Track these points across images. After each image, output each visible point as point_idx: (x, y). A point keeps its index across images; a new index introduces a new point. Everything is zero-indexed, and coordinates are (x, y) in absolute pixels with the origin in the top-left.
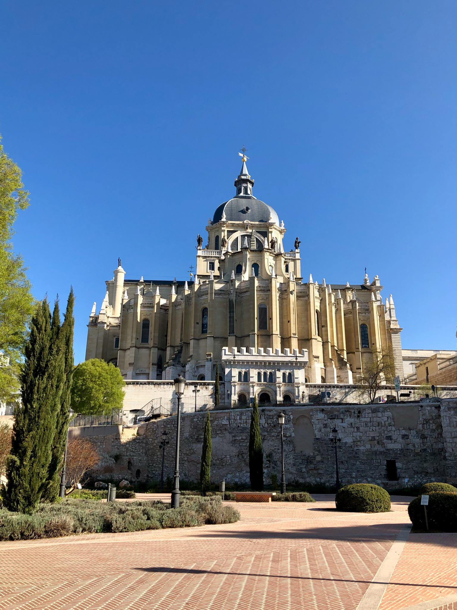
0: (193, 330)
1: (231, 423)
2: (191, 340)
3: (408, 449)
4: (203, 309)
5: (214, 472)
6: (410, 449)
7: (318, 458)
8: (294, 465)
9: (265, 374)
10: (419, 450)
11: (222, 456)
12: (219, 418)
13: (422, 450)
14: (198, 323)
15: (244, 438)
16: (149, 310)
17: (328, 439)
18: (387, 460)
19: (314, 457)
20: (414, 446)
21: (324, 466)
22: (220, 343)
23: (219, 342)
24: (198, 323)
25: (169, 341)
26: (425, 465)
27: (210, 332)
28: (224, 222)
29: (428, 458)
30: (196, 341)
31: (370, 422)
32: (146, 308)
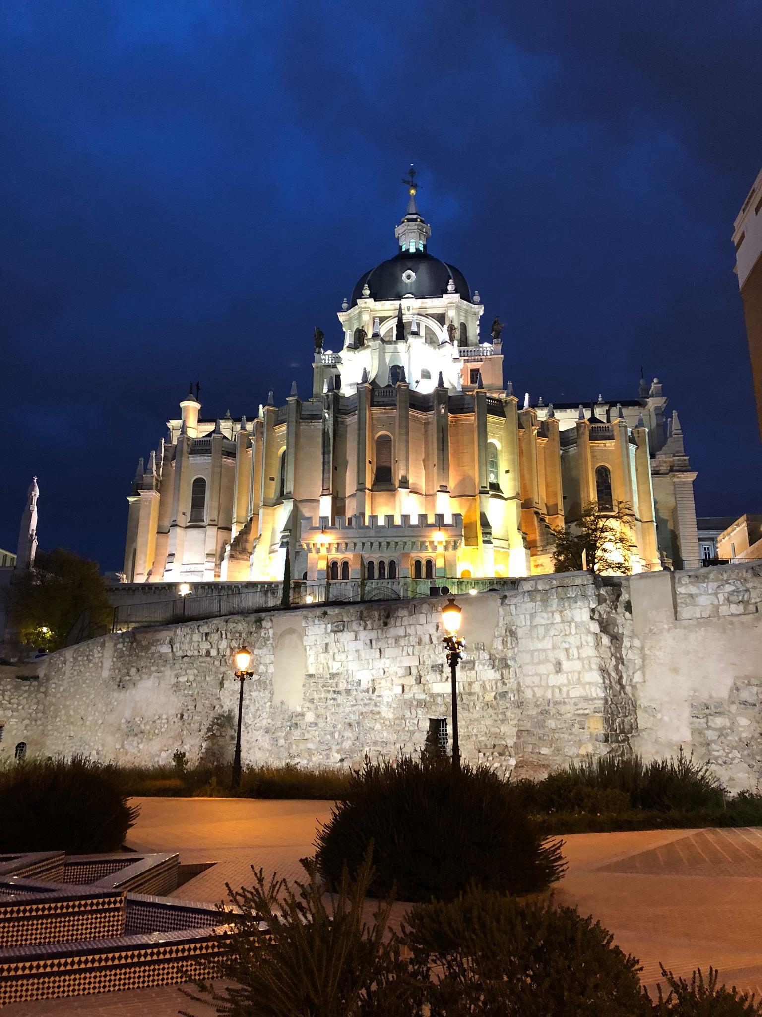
1: (174, 650)
3: (470, 694)
5: (141, 746)
6: (475, 693)
7: (310, 717)
8: (267, 732)
9: (382, 564)
10: (493, 694)
11: (155, 715)
12: (158, 640)
13: (500, 694)
14: (272, 479)
15: (192, 678)
17: (328, 676)
18: (431, 719)
19: (302, 715)
20: (484, 687)
21: (317, 733)
24: (272, 479)
25: (235, 516)
26: (503, 729)
29: (508, 714)
31: (405, 636)
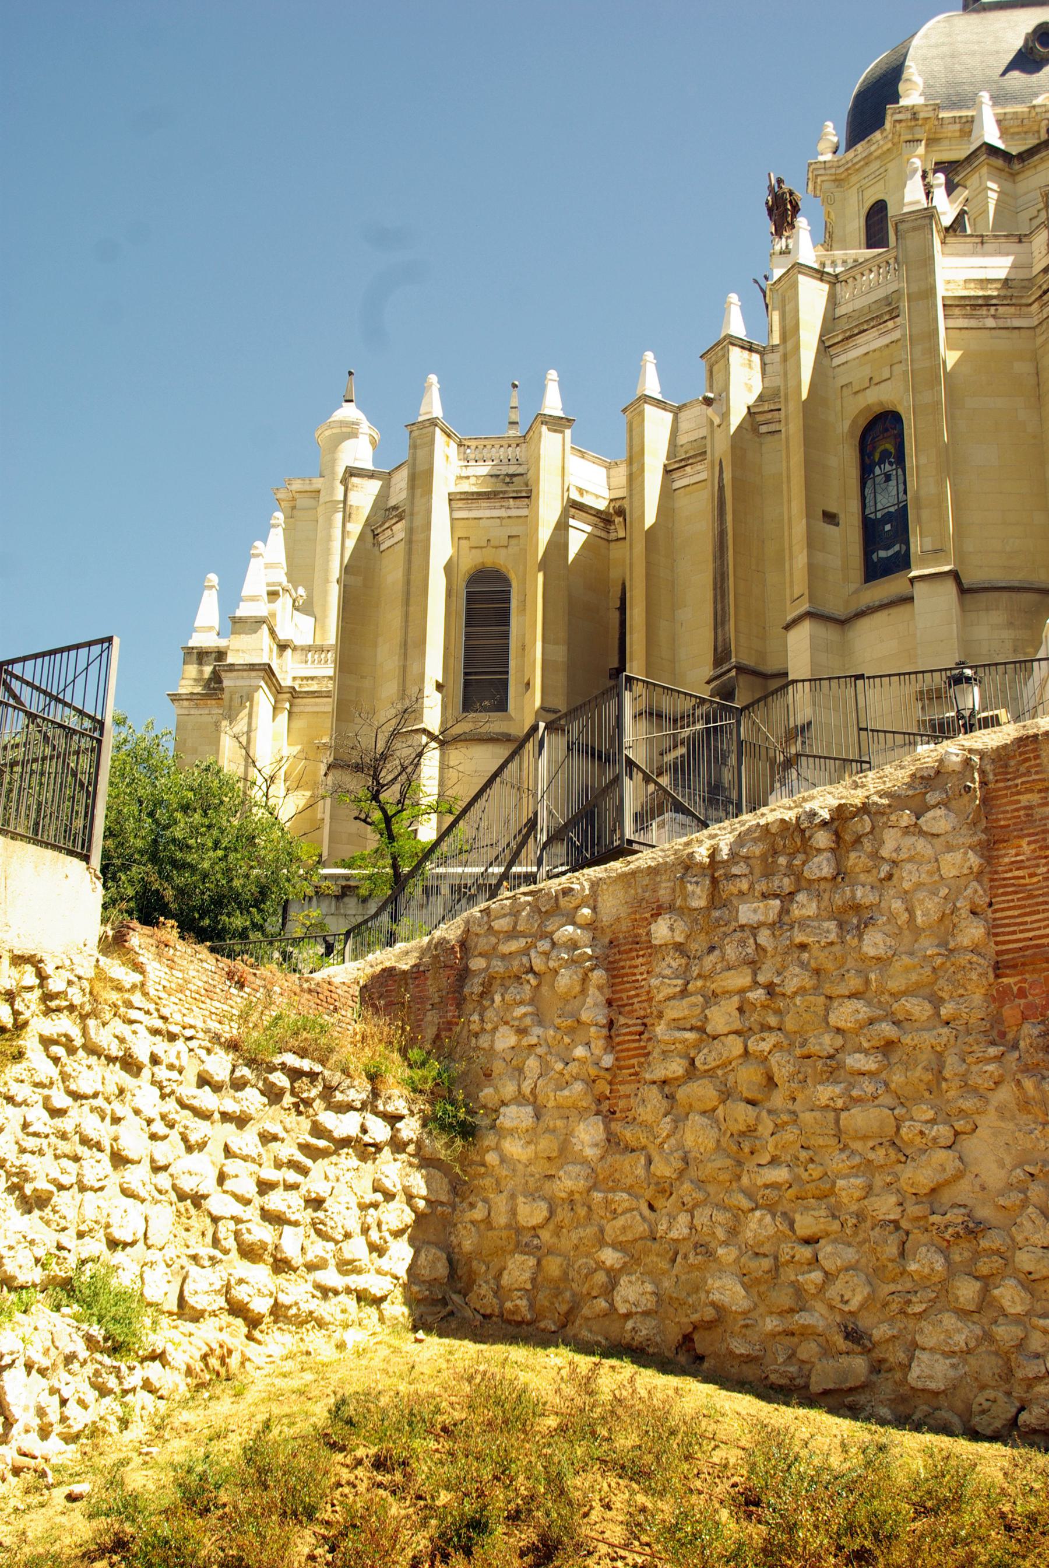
0: (800, 560)
2: (787, 627)
4: (863, 423)
14: (830, 518)
16: (502, 513)
22: (1011, 625)
23: (997, 617)
24: (830, 518)
27: (928, 547)
28: (914, 113)
30: (828, 633)
32: (484, 504)
